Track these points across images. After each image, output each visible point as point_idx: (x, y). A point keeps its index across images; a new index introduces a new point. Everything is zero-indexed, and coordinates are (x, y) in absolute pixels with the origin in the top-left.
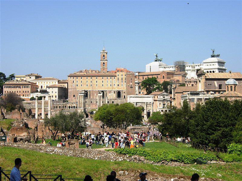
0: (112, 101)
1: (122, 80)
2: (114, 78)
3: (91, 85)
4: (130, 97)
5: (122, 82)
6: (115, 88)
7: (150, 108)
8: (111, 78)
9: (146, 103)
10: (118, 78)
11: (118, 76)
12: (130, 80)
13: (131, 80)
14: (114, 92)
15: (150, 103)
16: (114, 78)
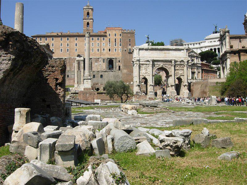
0: (100, 74)
1: (115, 42)
2: (104, 40)
3: (68, 49)
4: (140, 49)
5: (115, 45)
6: (104, 55)
7: (180, 72)
8: (98, 39)
9: (173, 62)
10: (110, 39)
11: (110, 36)
12: (127, 42)
13: (130, 41)
14: (104, 60)
15: (182, 61)
16: (104, 40)
